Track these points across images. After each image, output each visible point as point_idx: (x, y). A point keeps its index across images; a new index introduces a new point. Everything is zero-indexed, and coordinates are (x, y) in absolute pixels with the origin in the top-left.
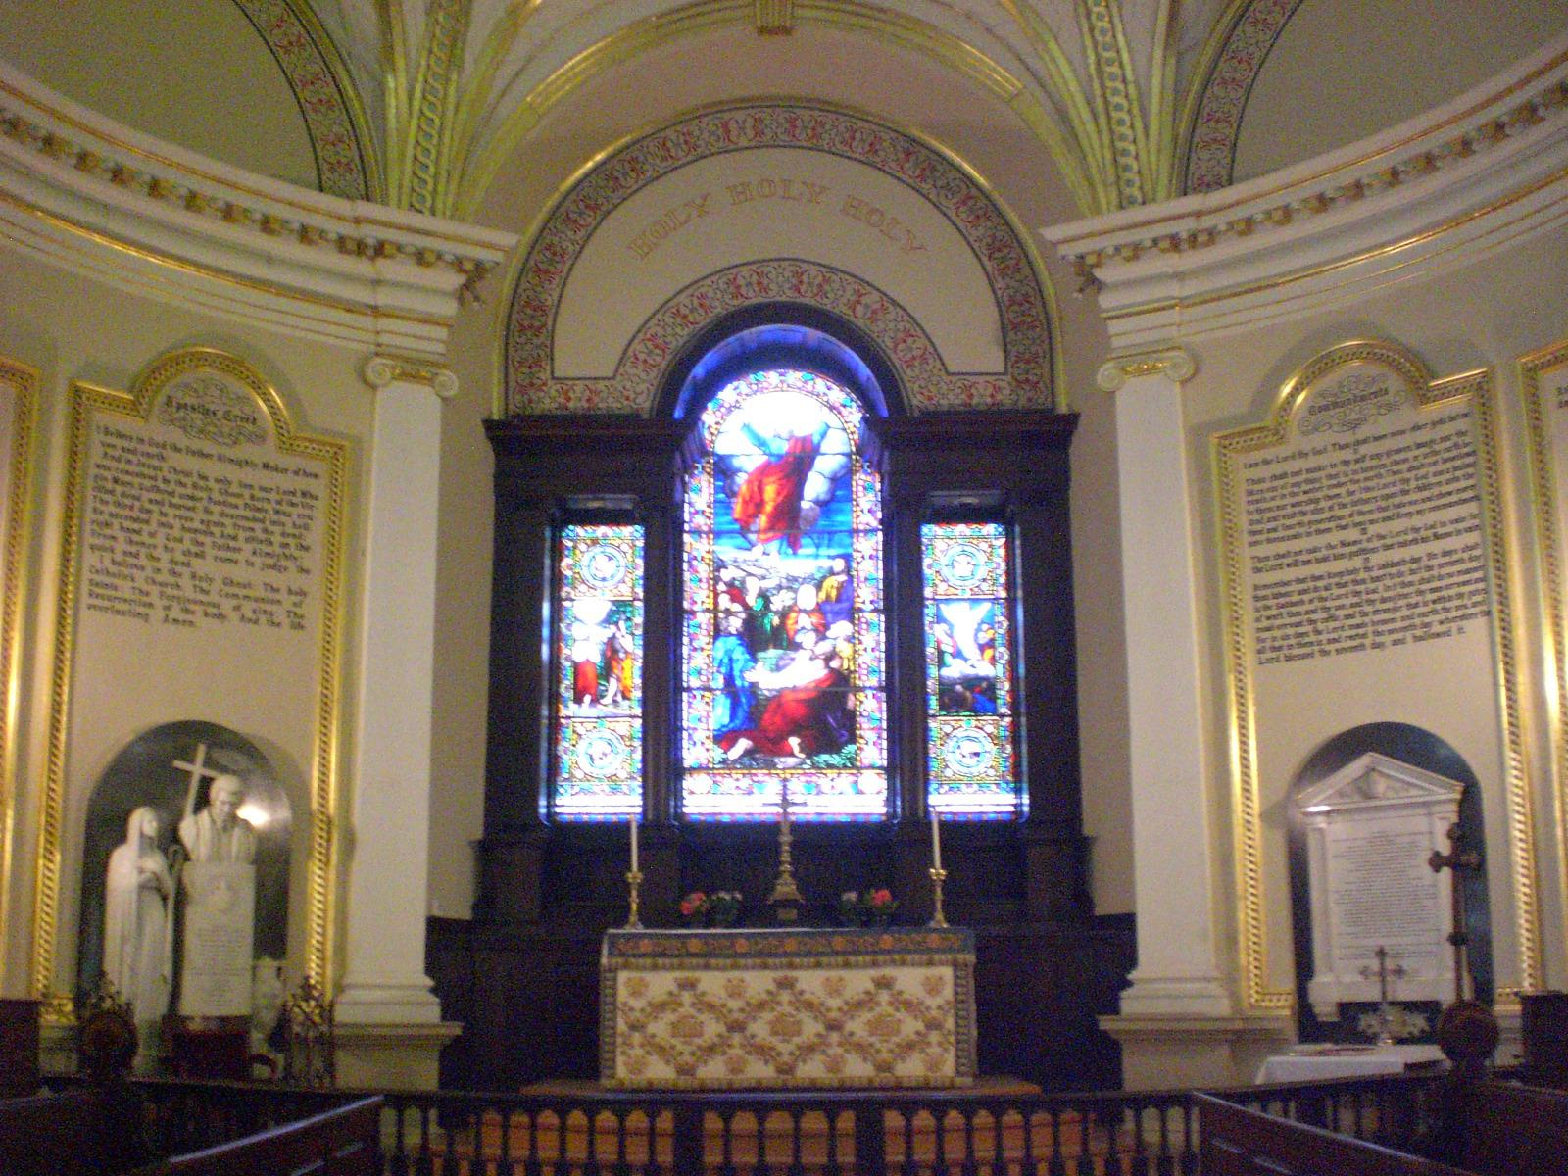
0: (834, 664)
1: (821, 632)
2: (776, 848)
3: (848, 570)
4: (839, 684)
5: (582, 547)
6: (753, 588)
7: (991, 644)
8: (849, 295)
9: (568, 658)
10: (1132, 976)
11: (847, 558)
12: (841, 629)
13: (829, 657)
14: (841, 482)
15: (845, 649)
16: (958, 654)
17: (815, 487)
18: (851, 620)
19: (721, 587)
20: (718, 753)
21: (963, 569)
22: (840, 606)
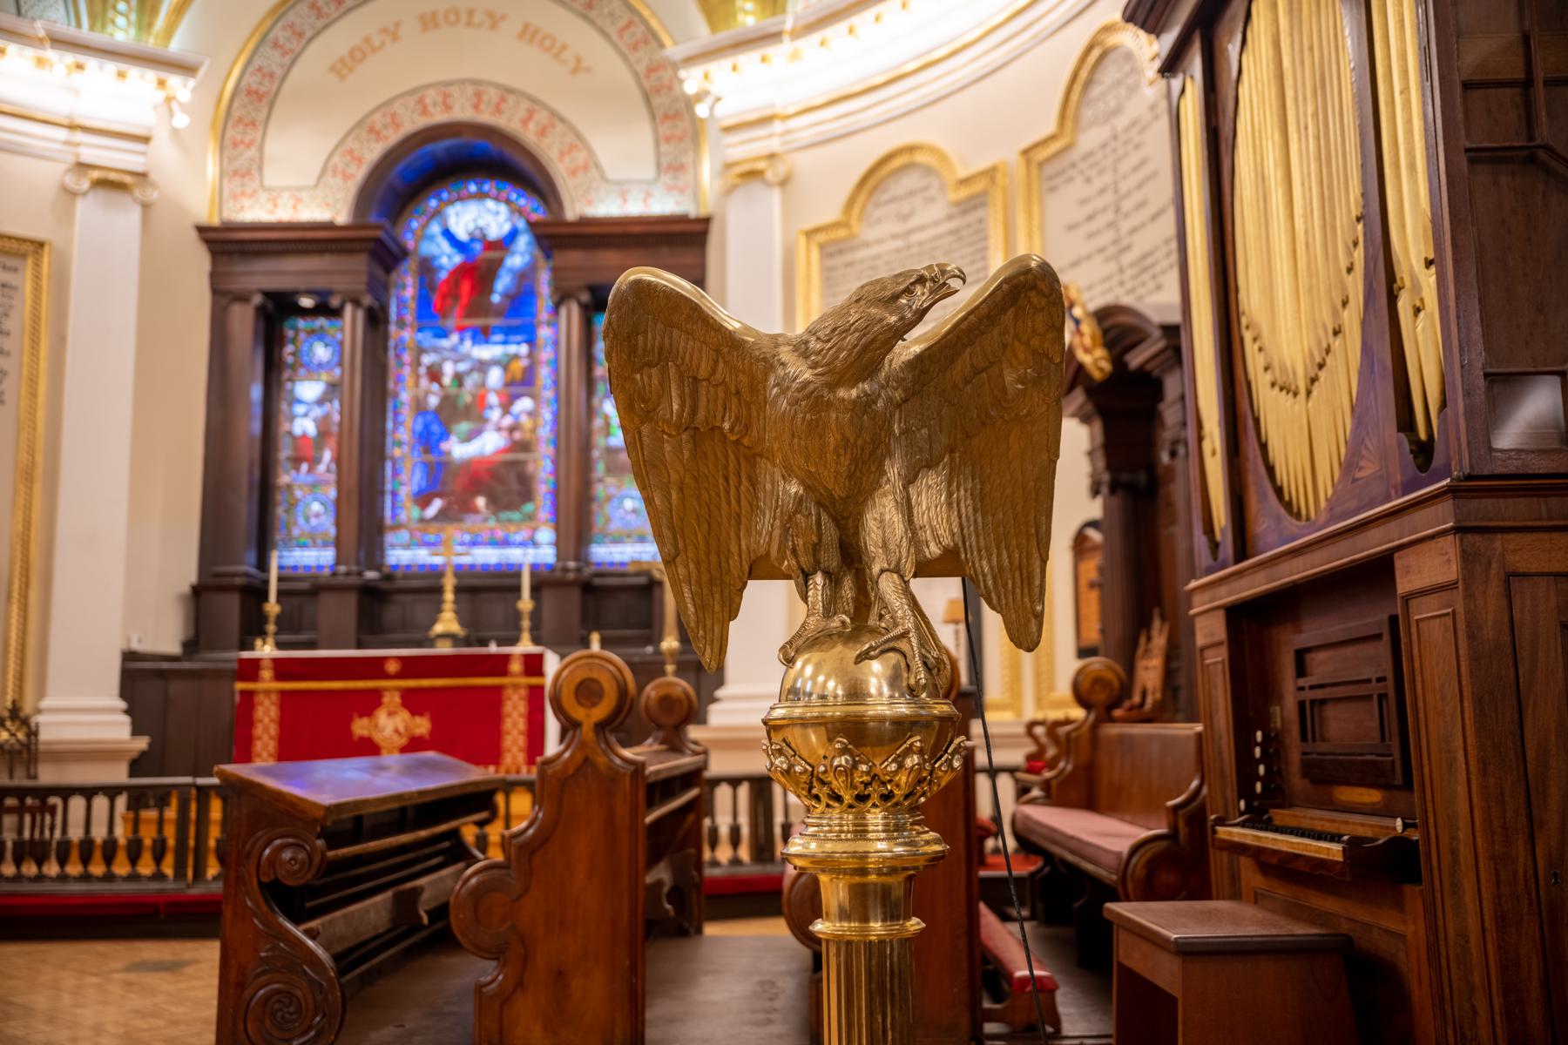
0: (517, 435)
1: (506, 408)
2: (438, 590)
3: (530, 355)
5: (302, 336)
6: (449, 369)
8: (522, 112)
9: (290, 433)
10: (720, 693)
12: (524, 404)
13: (512, 429)
14: (525, 278)
15: (525, 421)
17: (503, 283)
18: (532, 396)
19: (422, 371)
20: (415, 512)
22: (520, 384)
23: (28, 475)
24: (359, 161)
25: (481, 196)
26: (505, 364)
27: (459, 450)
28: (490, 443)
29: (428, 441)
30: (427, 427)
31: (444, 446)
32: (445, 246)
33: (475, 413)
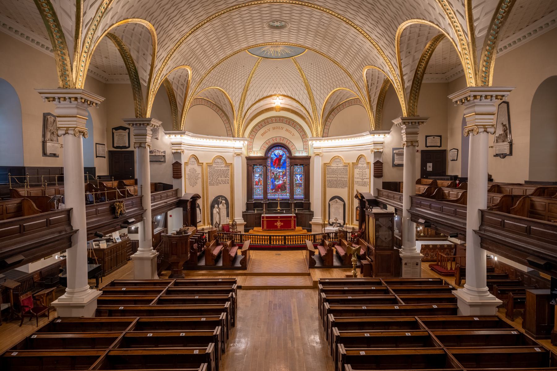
3: (286, 171)
6: (275, 172)
7: (301, 179)
11: (286, 169)
12: (285, 177)
13: (283, 181)
14: (285, 161)
16: (298, 180)
17: (282, 161)
20: (271, 191)
21: (299, 171)
22: (284, 175)
24: (265, 147)
28: (281, 182)
29: (273, 182)
30: (272, 180)
31: (275, 183)
33: (279, 179)
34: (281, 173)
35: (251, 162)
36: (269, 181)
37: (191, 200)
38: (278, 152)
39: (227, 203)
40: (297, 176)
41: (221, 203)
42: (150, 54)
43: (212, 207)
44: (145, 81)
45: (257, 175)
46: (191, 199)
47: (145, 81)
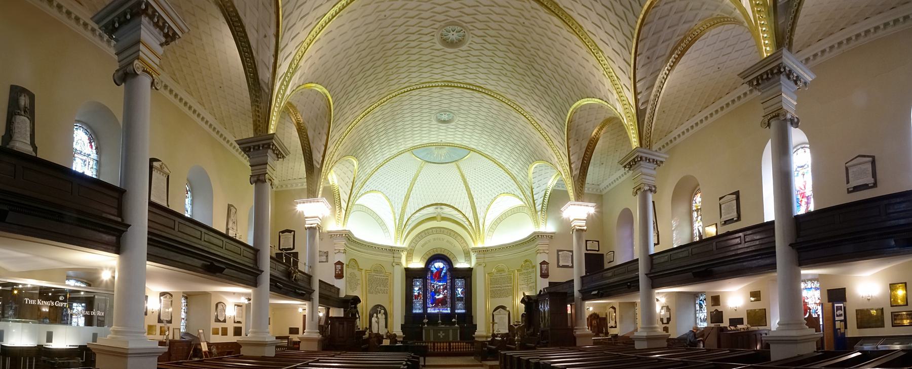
4: (445, 297)
12: (446, 291)
17: (442, 274)
21: (460, 284)
23: (390, 302)
25: (439, 262)
26: (443, 285)
27: (437, 297)
28: (441, 296)
32: (435, 269)
34: (442, 287)
35: (411, 275)
36: (429, 295)
37: (352, 301)
38: (439, 265)
39: (386, 313)
40: (458, 289)
41: (380, 313)
42: (325, 133)
43: (371, 316)
44: (318, 163)
45: (416, 289)
46: (352, 299)
47: (318, 163)
